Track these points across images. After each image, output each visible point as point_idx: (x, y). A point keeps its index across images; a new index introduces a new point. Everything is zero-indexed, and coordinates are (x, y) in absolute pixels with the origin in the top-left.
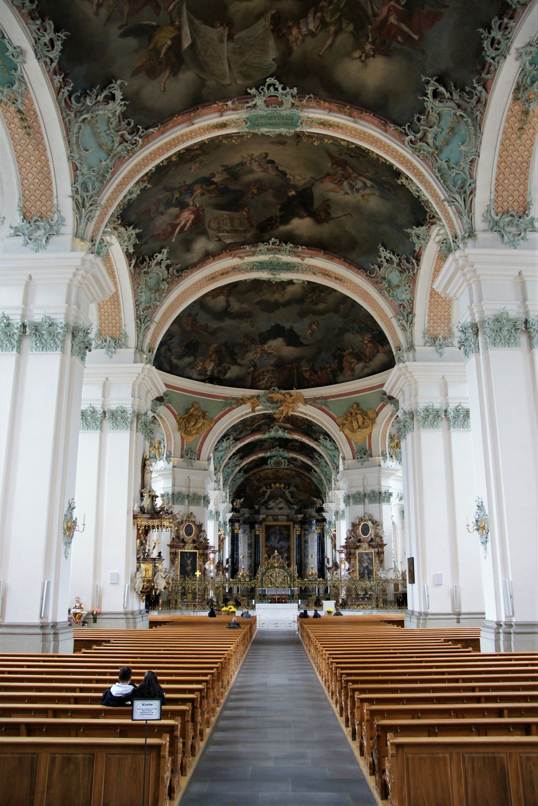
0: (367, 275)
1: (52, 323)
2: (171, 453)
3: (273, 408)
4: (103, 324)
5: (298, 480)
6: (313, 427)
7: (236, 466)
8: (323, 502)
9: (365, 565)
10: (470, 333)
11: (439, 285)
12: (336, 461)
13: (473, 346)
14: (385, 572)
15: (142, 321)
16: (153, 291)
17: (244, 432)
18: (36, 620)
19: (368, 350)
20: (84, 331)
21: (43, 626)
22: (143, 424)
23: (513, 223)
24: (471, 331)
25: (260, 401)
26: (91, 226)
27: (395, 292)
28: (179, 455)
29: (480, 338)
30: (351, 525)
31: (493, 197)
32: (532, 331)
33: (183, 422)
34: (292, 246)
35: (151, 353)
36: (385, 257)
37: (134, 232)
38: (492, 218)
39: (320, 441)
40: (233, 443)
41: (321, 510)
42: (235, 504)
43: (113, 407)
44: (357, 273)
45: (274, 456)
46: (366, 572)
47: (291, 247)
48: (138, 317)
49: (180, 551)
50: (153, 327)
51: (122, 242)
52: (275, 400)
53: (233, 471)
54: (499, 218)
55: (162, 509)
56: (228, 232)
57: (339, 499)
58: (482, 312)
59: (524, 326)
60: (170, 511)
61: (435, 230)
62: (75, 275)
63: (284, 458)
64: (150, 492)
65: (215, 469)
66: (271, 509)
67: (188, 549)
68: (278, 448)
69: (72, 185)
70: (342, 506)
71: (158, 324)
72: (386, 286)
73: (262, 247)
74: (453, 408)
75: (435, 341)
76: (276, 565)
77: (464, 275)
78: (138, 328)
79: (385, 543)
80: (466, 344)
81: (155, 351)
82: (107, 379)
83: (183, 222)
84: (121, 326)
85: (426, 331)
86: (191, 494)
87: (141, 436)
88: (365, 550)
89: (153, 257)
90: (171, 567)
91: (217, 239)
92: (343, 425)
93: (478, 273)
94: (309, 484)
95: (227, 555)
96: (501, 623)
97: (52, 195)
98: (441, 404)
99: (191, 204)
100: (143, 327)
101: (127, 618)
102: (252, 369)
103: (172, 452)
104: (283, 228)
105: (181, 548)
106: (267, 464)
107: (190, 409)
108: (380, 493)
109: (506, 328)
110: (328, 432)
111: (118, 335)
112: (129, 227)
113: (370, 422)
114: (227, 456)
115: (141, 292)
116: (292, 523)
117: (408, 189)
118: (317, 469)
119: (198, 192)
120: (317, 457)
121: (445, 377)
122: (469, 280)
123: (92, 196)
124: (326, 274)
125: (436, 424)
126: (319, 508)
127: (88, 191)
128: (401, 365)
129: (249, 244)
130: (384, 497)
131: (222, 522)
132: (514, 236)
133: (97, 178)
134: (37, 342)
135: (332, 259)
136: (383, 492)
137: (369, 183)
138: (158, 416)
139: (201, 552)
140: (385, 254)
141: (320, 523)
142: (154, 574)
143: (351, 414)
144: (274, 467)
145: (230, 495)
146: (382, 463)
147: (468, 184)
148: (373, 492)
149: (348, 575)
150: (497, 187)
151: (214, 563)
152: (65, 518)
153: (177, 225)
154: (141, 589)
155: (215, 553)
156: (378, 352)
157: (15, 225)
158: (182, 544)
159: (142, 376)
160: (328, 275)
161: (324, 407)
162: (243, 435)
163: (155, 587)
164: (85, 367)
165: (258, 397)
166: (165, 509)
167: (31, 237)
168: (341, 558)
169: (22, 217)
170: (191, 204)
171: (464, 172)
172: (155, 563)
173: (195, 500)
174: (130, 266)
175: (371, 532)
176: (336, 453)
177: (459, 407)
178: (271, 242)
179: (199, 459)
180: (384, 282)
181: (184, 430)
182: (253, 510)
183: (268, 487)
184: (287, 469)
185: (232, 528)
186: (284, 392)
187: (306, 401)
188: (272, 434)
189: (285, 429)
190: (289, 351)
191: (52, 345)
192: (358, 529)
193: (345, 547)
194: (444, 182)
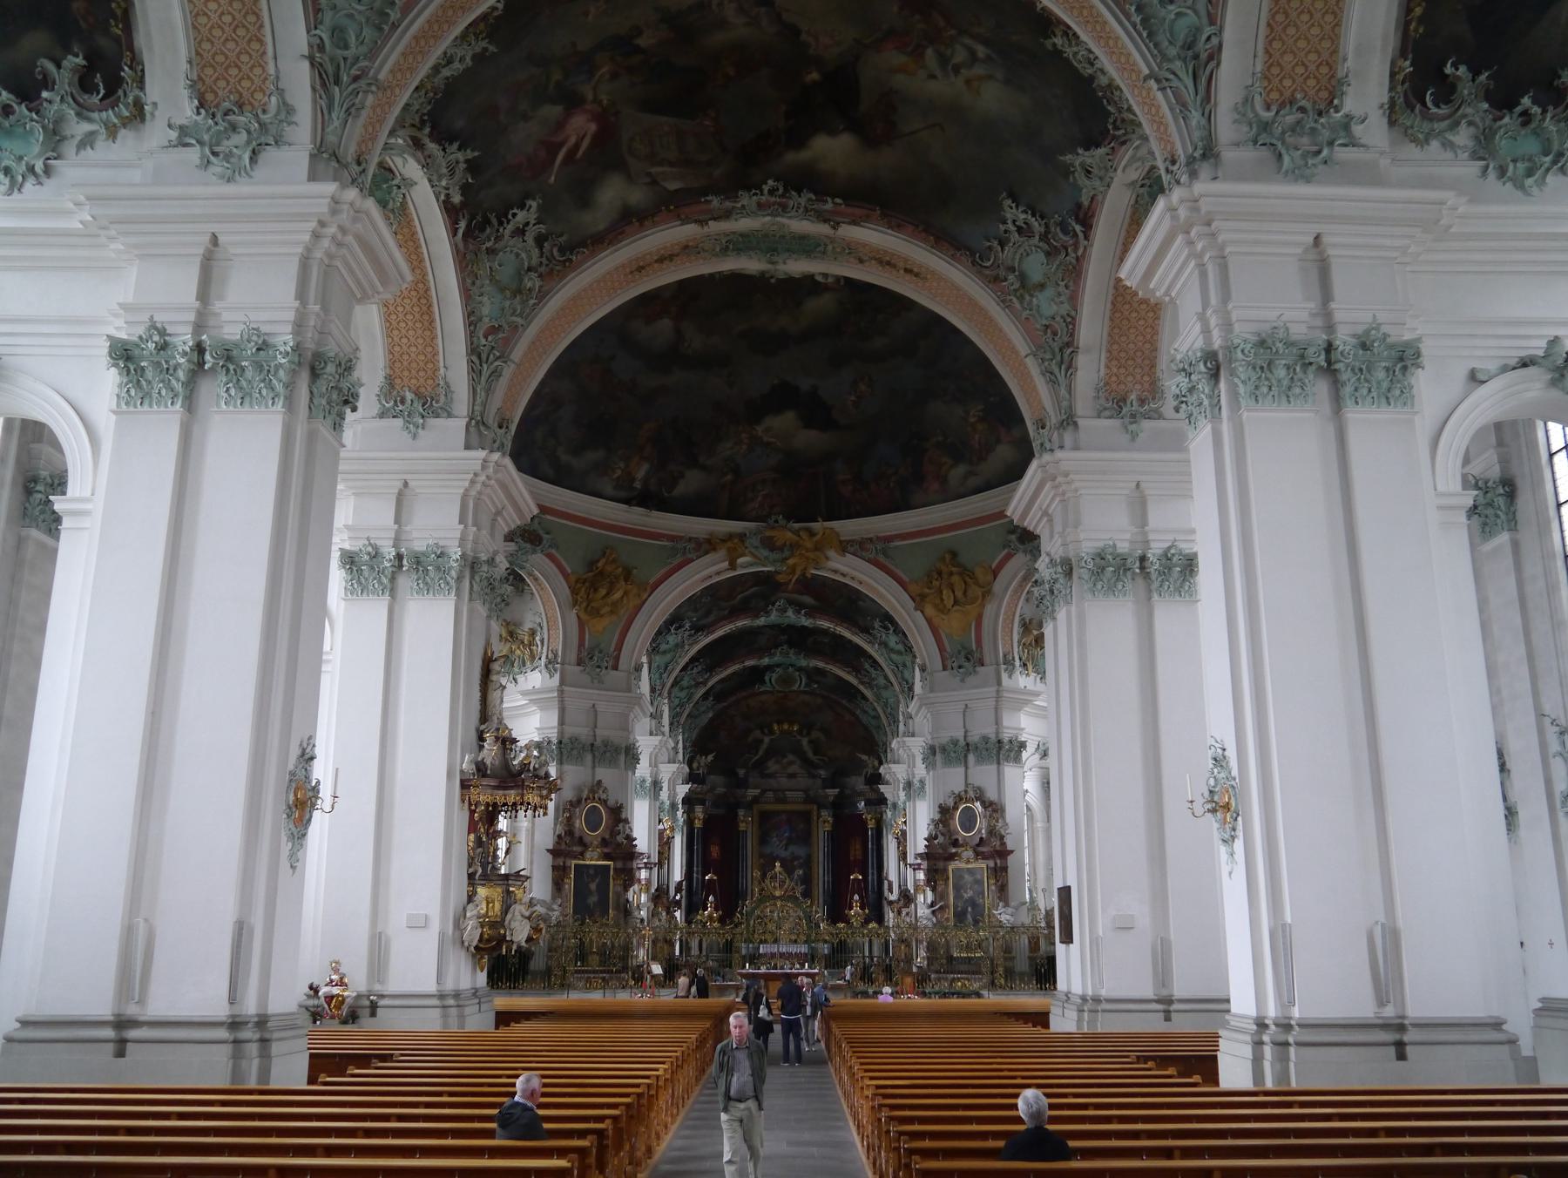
0: (974, 263)
1: (264, 342)
2: (556, 656)
3: (774, 562)
4: (398, 365)
6: (861, 603)
7: (698, 685)
8: (881, 763)
9: (968, 894)
10: (1200, 373)
11: (1131, 272)
12: (907, 674)
13: (1206, 402)
14: (1010, 910)
15: (484, 357)
16: (508, 293)
18: (221, 1011)
19: (977, 437)
20: (340, 364)
21: (235, 1024)
22: (486, 583)
23: (1303, 127)
24: (1202, 367)
25: (747, 544)
26: (357, 128)
27: (1034, 299)
28: (573, 657)
29: (1222, 385)
30: (937, 809)
31: (1259, 68)
32: (1343, 369)
33: (583, 589)
34: (814, 198)
35: (503, 430)
36: (1014, 221)
37: (460, 156)
38: (1257, 115)
39: (875, 632)
40: (690, 635)
41: (876, 779)
42: (695, 765)
43: (419, 546)
44: (953, 257)
45: (778, 665)
46: (969, 909)
47: (810, 200)
48: (473, 350)
49: (574, 862)
50: (508, 371)
51: (435, 178)
52: (778, 544)
54: (1272, 114)
55: (524, 767)
56: (671, 164)
57: (914, 756)
58: (1227, 326)
59: (1323, 357)
60: (542, 773)
61: (1127, 154)
62: (316, 236)
63: (800, 669)
64: (498, 729)
65: (653, 690)
66: (770, 776)
67: (593, 860)
68: (785, 647)
69: (308, 32)
70: (920, 770)
71: (518, 366)
72: (1017, 285)
73: (746, 200)
74: (1159, 552)
75: (1121, 407)
77: (1190, 243)
78: (474, 371)
79: (1009, 848)
80: (1192, 399)
81: (513, 428)
82: (406, 484)
83: (573, 140)
84: (437, 370)
85: (1102, 384)
86: (598, 743)
87: (482, 611)
88: (968, 862)
89: (507, 218)
90: (554, 898)
91: (648, 180)
92: (923, 597)
93: (1221, 238)
95: (677, 875)
96: (1267, 1022)
97: (264, 53)
98: (1131, 542)
99: (590, 97)
100: (486, 373)
101: (444, 1007)
102: (729, 477)
103: (560, 653)
104: (792, 157)
105: (575, 858)
106: (763, 682)
107: (598, 561)
108: (999, 742)
109: (1284, 362)
110: (891, 613)
111: (429, 388)
112: (451, 143)
113: (977, 591)
115: (482, 295)
116: (815, 807)
117: (1067, 59)
118: (868, 693)
119: (605, 69)
120: (867, 666)
121: (1143, 485)
122: (1200, 256)
123: (357, 59)
124: (886, 261)
125: (1120, 587)
127: (346, 47)
128: (1047, 457)
129: (716, 194)
130: (1010, 750)
131: (668, 803)
132: (1305, 156)
133: (368, 20)
134: (230, 385)
135: (897, 227)
136: (1006, 740)
137: (981, 51)
138: (530, 574)
139: (620, 865)
140: (1014, 214)
141: (873, 808)
142: (506, 910)
143: (940, 573)
144: (777, 688)
146: (1004, 676)
147: (1204, 37)
148: (985, 739)
149: (931, 916)
150: (1270, 43)
151: (648, 890)
152: (291, 781)
153: (561, 144)
154: (475, 943)
155: (651, 868)
156: (998, 441)
157: (179, 121)
158: (577, 849)
159: (483, 478)
160: (888, 263)
161: (881, 558)
162: (711, 618)
163: (508, 938)
164: (344, 446)
165: (742, 537)
166: (531, 768)
167: (216, 149)
168: (915, 881)
169: (196, 102)
170: (590, 97)
171: (1196, 12)
172: (509, 885)
173: (608, 754)
174: (455, 234)
175: (981, 825)
176: (908, 659)
177: (1173, 551)
178: (766, 188)
179: (615, 668)
180: (1011, 278)
181: (585, 604)
183: (766, 731)
184: (805, 692)
186: (797, 525)
187: (844, 547)
188: (774, 617)
189: (799, 607)
190: (808, 439)
191: (264, 392)
192: (952, 818)
193: (929, 856)
194: (1150, 35)
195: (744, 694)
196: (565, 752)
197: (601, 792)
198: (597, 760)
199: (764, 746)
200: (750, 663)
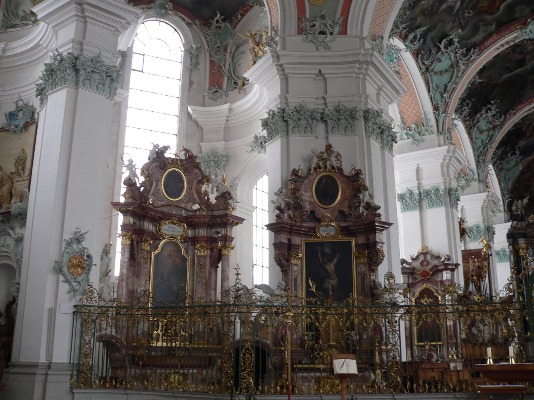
7: (494, 128)
17: (482, 29)
42: (514, 208)
53: (491, 138)
65: (436, 108)
114: (457, 83)
139: (362, 240)
145: (503, 195)
155: (452, 270)
173: (343, 122)
185: (513, 247)
196: (290, 122)
197: (333, 159)
198: (330, 128)
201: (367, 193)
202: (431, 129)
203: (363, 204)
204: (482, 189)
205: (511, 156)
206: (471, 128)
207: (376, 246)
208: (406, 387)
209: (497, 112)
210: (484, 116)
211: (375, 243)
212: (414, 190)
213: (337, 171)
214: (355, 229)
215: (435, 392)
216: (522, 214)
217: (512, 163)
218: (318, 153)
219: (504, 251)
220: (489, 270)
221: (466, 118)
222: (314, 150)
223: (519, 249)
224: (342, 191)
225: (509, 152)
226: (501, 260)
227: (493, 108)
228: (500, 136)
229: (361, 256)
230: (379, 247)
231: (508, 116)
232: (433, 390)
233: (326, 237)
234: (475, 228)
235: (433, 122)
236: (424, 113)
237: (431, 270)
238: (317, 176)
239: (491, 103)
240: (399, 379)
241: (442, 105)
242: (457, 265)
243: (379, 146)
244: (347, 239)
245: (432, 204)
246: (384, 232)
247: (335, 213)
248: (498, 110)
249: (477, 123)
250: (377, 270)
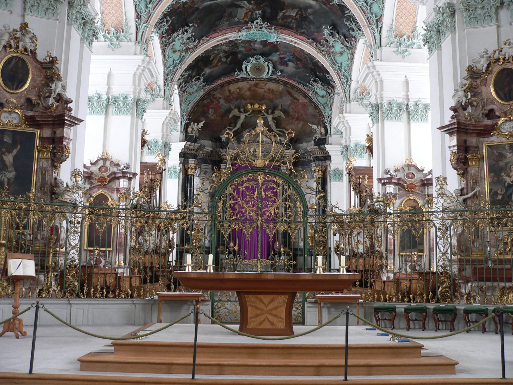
5: (286, 101)
12: (375, 8)
41: (322, 142)
42: (189, 130)
53: (182, 59)
65: (138, 17)
68: (259, 20)
76: (259, 163)
94: (304, 105)
106: (241, 70)
120: (327, 32)
126: (319, 138)
139: (47, 133)
144: (251, 75)
145: (182, 116)
155: (130, 179)
182: (218, 144)
183: (242, 110)
184: (270, 80)
185: (184, 166)
192: (485, 83)
195: (227, 79)
197: (27, 40)
199: (241, 121)
200: (232, 36)
201: (60, 83)
202: (130, 36)
203: (54, 95)
204: (165, 106)
205: (196, 81)
206: (166, 45)
207: (62, 141)
208: (83, 292)
209: (192, 35)
210: (180, 36)
211: (62, 138)
212: (102, 95)
213: (30, 54)
214: (42, 121)
215: (112, 298)
216: (196, 136)
217: (195, 88)
218: (11, 30)
219: (175, 168)
220: (160, 184)
221: (163, 34)
222: (6, 26)
223: (189, 168)
224: (32, 77)
225: (195, 76)
226: (171, 176)
227: (190, 30)
228: (190, 58)
229: (45, 150)
230: (65, 143)
231: (201, 41)
232: (111, 295)
233: (7, 124)
234: (154, 143)
235: (133, 30)
236: (126, 19)
237: (108, 177)
238: (6, 55)
239: (189, 26)
240: (76, 283)
241: (146, 15)
242: (135, 175)
243: (80, 38)
244: (30, 130)
245: (119, 111)
246: (72, 128)
247: (22, 100)
248: (193, 34)
249: (172, 42)
250: (60, 167)
